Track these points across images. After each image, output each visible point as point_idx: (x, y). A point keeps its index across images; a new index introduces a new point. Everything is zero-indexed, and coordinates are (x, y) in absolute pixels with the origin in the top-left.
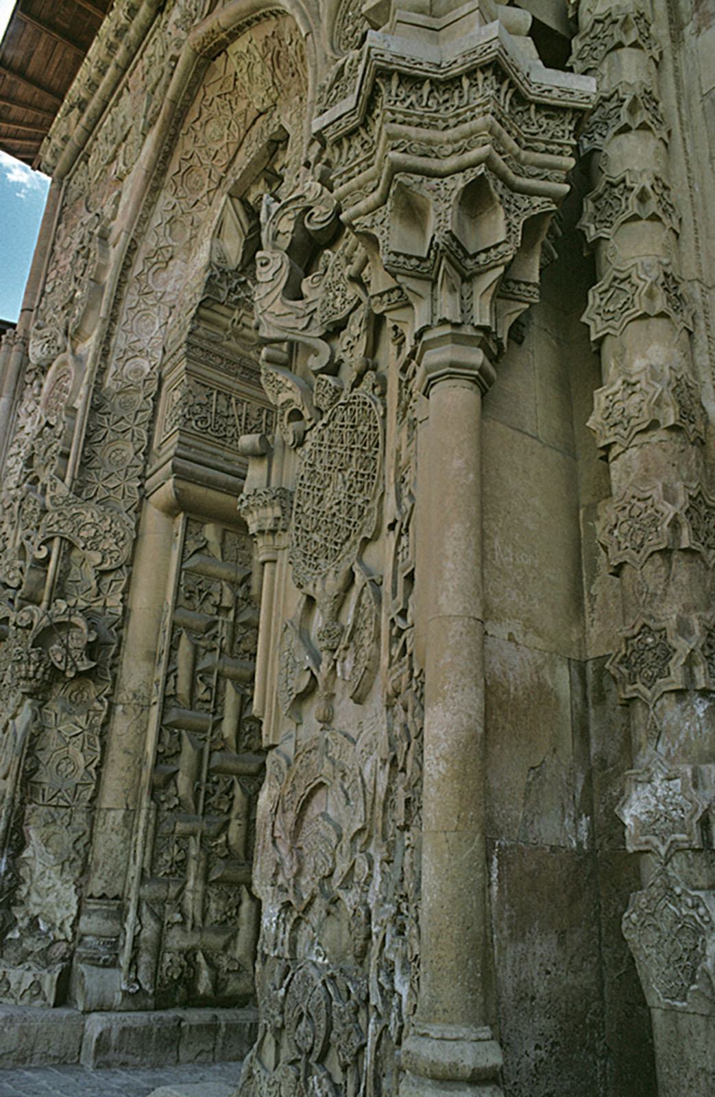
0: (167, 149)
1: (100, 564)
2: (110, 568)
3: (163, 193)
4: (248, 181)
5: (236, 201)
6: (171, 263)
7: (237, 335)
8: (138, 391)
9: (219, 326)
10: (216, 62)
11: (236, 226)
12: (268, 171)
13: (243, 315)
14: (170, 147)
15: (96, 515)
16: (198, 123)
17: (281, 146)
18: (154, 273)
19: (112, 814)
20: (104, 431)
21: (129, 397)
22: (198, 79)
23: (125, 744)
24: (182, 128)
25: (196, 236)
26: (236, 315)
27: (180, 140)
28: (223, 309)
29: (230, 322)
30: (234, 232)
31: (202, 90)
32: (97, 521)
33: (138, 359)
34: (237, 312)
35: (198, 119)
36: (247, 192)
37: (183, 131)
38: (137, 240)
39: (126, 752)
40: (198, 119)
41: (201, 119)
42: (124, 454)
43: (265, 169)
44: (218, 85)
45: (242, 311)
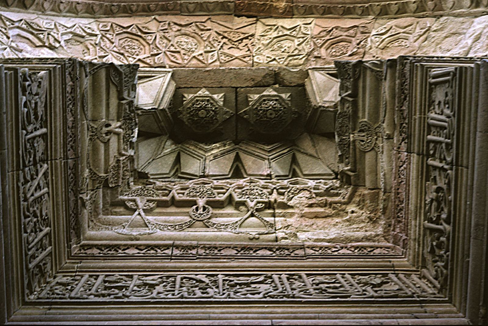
0: (134, 9)
3: (92, 20)
5: (173, 85)
7: (95, 136)
9: (94, 106)
10: (236, 18)
11: (159, 93)
12: (236, 93)
13: (118, 134)
14: (136, 11)
16: (178, 28)
22: (213, 10)
24: (160, 15)
26: (115, 125)
27: (149, 19)
28: (114, 101)
30: (154, 93)
31: (207, 18)
34: (119, 124)
35: (180, 25)
37: (157, 17)
38: (34, 7)
40: (180, 25)
41: (183, 28)
43: (237, 88)
44: (222, 29)
45: (121, 130)
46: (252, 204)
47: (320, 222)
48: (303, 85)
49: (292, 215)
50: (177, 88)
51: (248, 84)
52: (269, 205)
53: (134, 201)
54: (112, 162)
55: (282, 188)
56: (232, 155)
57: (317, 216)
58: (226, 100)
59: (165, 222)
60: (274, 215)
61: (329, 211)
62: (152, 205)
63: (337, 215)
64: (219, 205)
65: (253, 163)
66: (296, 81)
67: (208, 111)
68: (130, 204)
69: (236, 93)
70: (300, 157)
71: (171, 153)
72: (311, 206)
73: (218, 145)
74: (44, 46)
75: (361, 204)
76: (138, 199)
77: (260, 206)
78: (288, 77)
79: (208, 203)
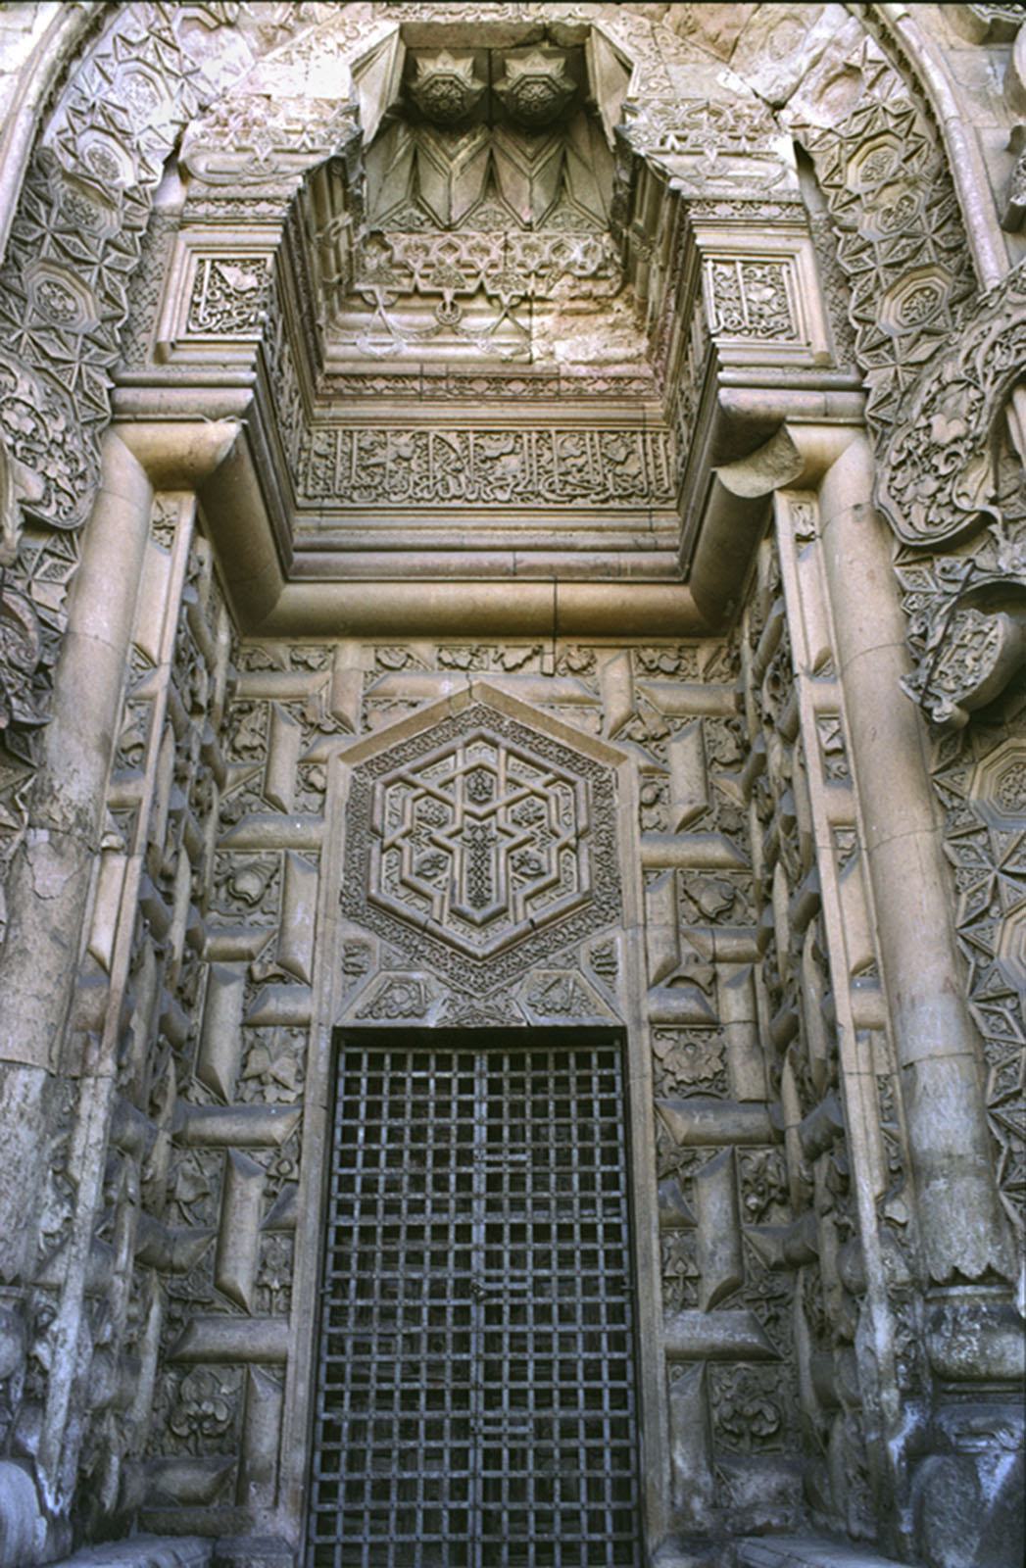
1: (38, 503)
2: (53, 521)
4: (450, 40)
6: (226, 31)
8: (109, 203)
12: (490, 57)
15: (36, 393)
17: (546, 45)
18: (185, 19)
19: (22, 1076)
20: (39, 232)
21: (81, 198)
23: (55, 920)
25: (291, 32)
29: (331, 222)
30: (377, 89)
32: (39, 409)
33: (111, 142)
36: (432, 52)
39: (55, 937)
42: (70, 305)
43: (490, 50)
46: (505, 300)
47: (581, 321)
48: (582, 47)
49: (550, 311)
50: (409, 49)
51: (506, 44)
52: (525, 299)
53: (372, 292)
54: (344, 258)
55: (543, 266)
56: (484, 158)
57: (578, 313)
58: (476, 72)
59: (410, 325)
60: (530, 312)
61: (592, 306)
62: (393, 298)
63: (601, 311)
64: (470, 297)
65: (512, 177)
66: (572, 41)
67: (452, 101)
68: (368, 297)
69: (490, 57)
70: (572, 161)
71: (406, 153)
72: (573, 299)
73: (464, 140)
74: (220, 24)
75: (629, 302)
76: (376, 289)
77: (515, 301)
78: (562, 34)
79: (457, 296)
